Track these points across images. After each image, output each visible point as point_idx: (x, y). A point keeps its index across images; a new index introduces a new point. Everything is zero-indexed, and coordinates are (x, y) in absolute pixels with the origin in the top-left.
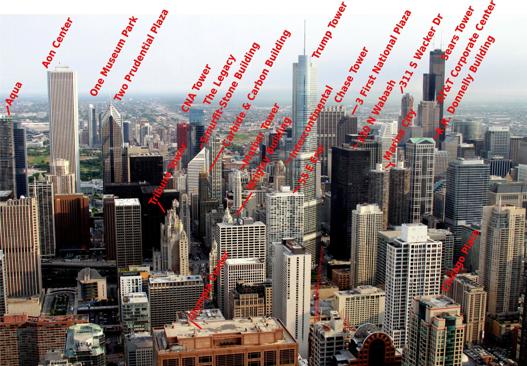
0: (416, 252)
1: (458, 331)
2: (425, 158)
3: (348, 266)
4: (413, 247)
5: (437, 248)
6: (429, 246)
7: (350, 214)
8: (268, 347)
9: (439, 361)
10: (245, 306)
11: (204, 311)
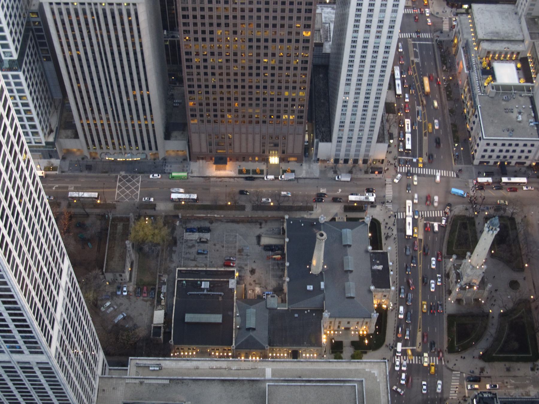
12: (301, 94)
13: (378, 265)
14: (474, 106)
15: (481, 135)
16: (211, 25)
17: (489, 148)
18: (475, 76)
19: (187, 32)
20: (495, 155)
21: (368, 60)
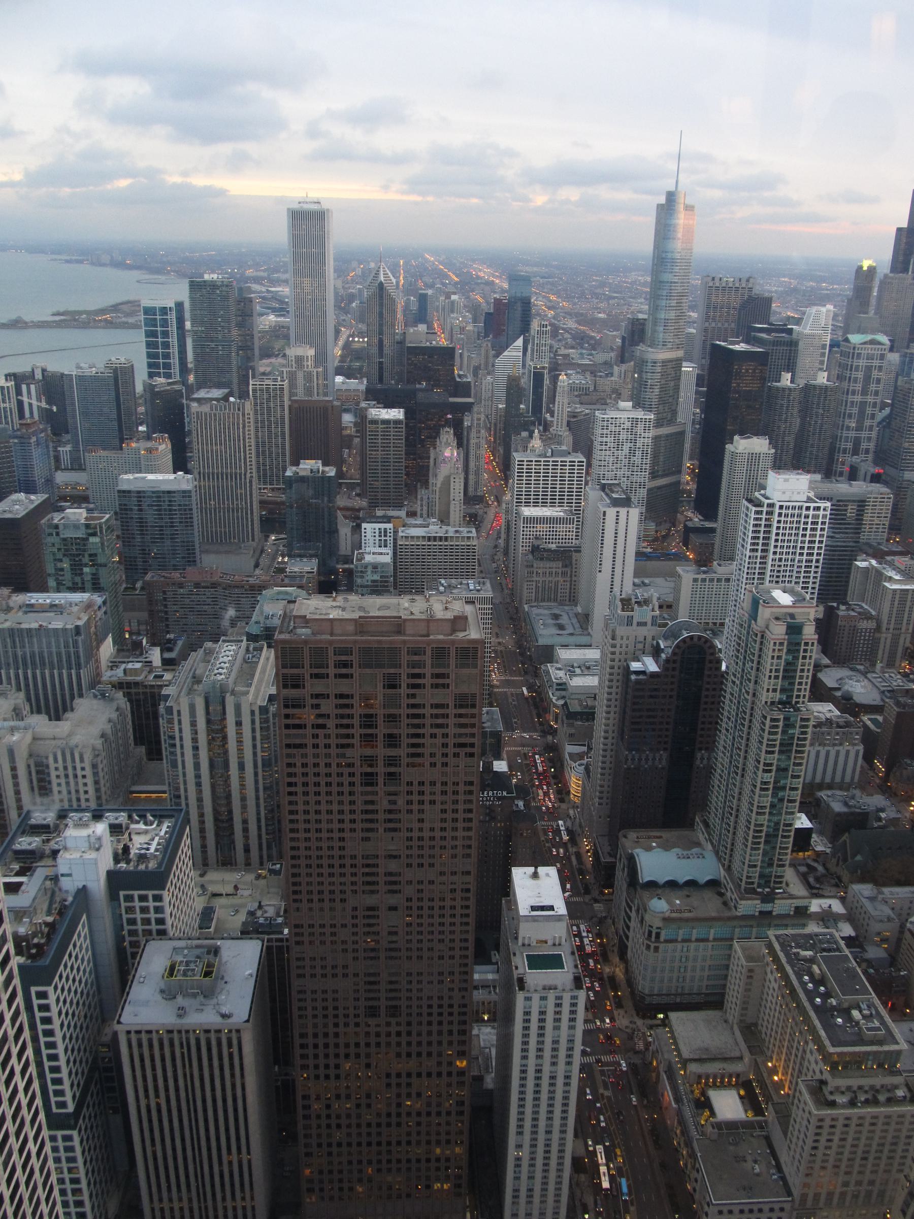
0: (786, 515)
1: (806, 644)
2: (869, 369)
3: (712, 530)
4: (781, 507)
5: (821, 513)
6: (808, 508)
7: (723, 450)
8: (439, 641)
9: (771, 688)
10: (541, 579)
11: (465, 582)
12: (457, 1150)
14: (692, 1155)
16: (337, 1056)
18: (688, 1112)
19: (304, 1067)
21: (544, 1096)
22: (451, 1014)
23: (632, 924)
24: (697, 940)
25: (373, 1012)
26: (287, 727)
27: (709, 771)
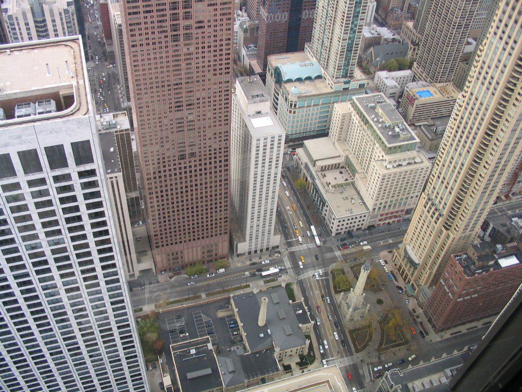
13: (299, 310)
15: (333, 217)
17: (340, 224)
20: (343, 227)
22: (220, 153)
23: (279, 102)
24: (315, 105)
25: (182, 157)
26: (130, 14)
27: (311, 21)
